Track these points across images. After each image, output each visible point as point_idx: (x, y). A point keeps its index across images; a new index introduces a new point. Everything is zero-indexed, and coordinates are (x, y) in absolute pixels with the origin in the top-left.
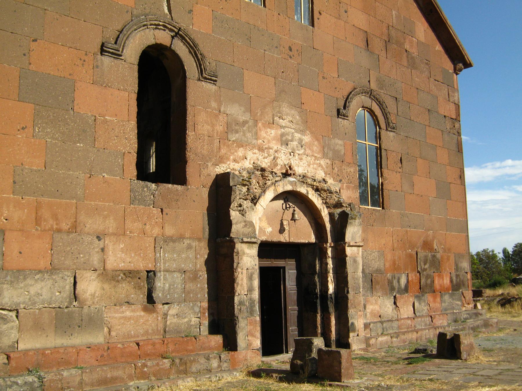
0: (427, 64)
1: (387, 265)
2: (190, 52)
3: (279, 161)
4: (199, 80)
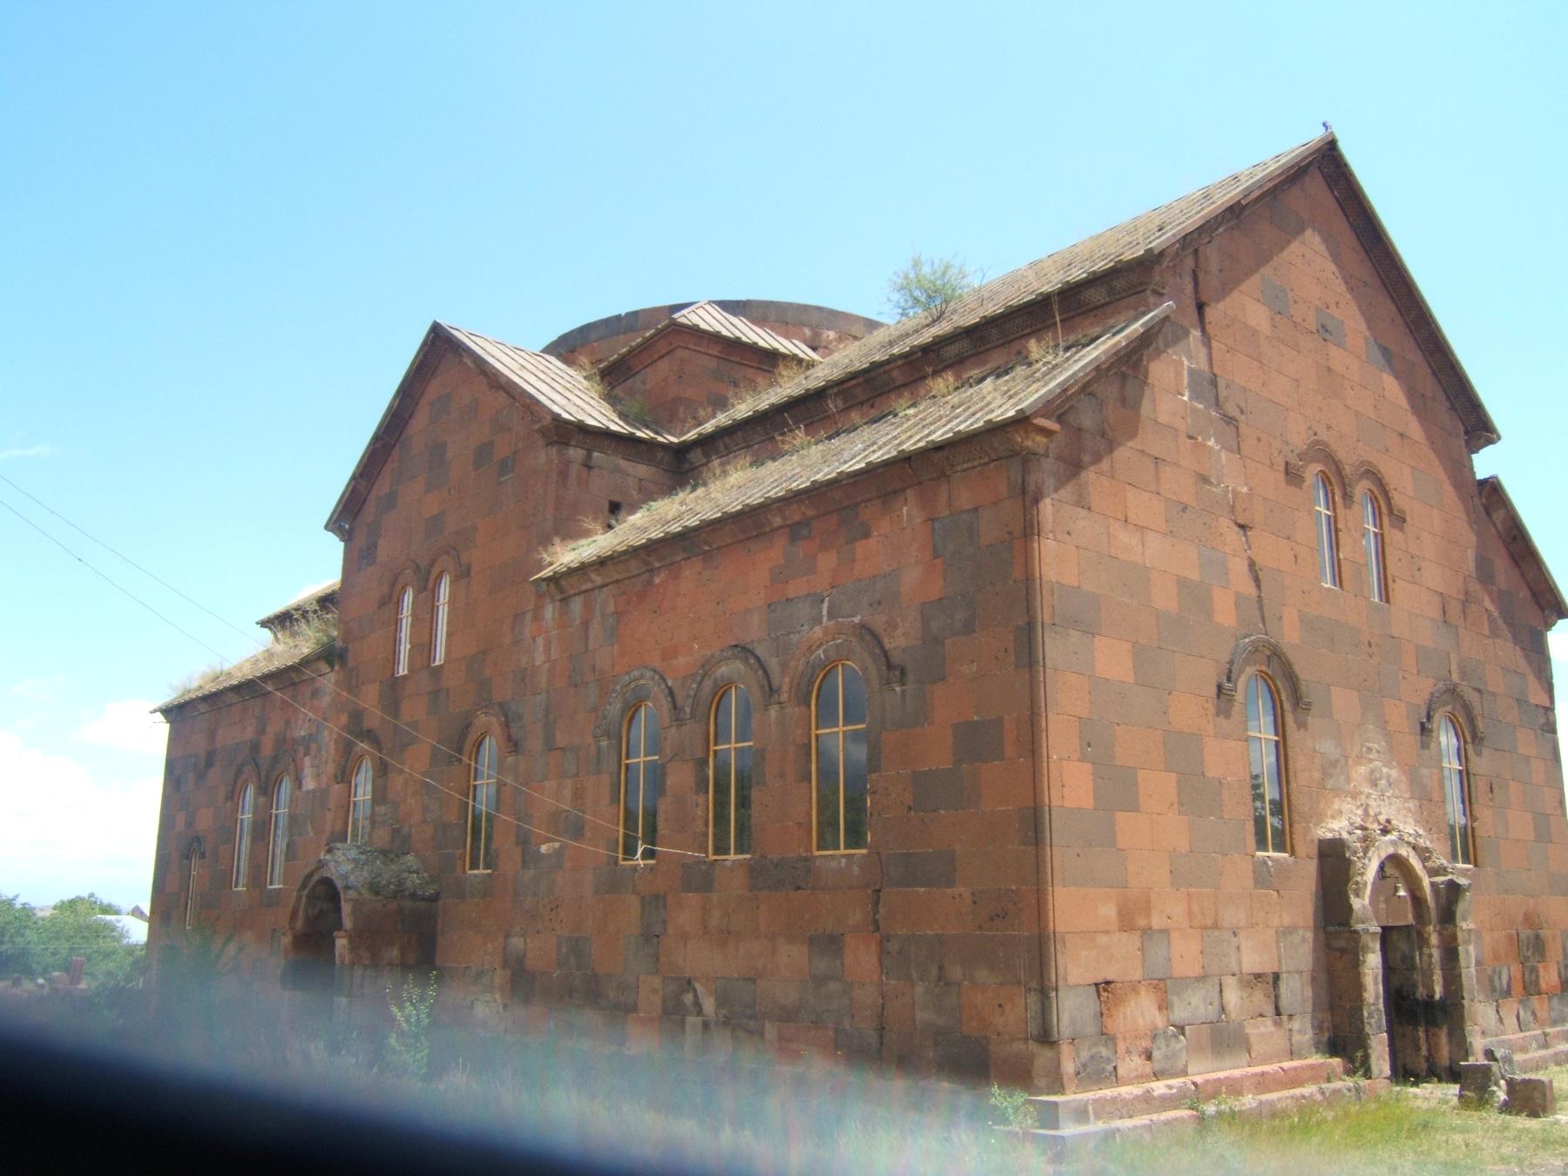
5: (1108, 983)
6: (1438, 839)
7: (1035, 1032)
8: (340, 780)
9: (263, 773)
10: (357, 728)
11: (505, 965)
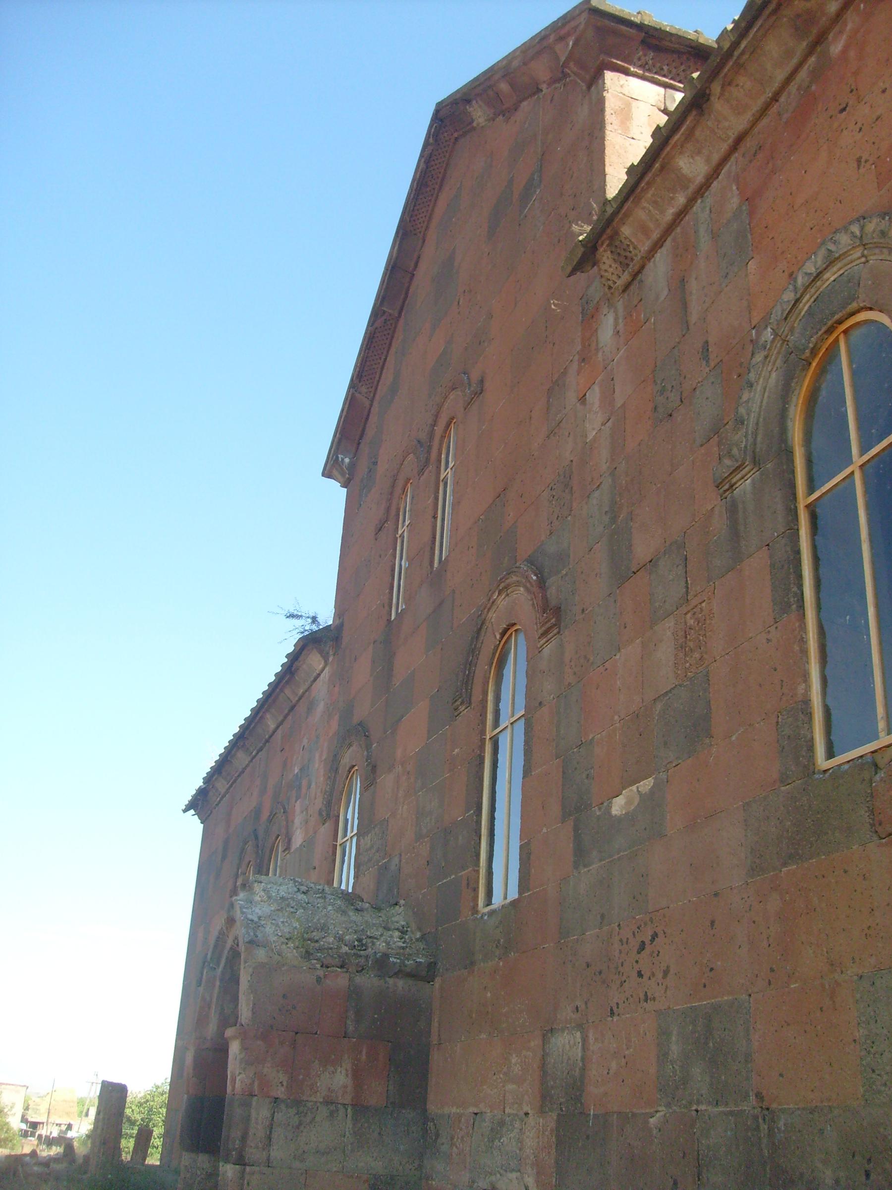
11: (545, 1099)
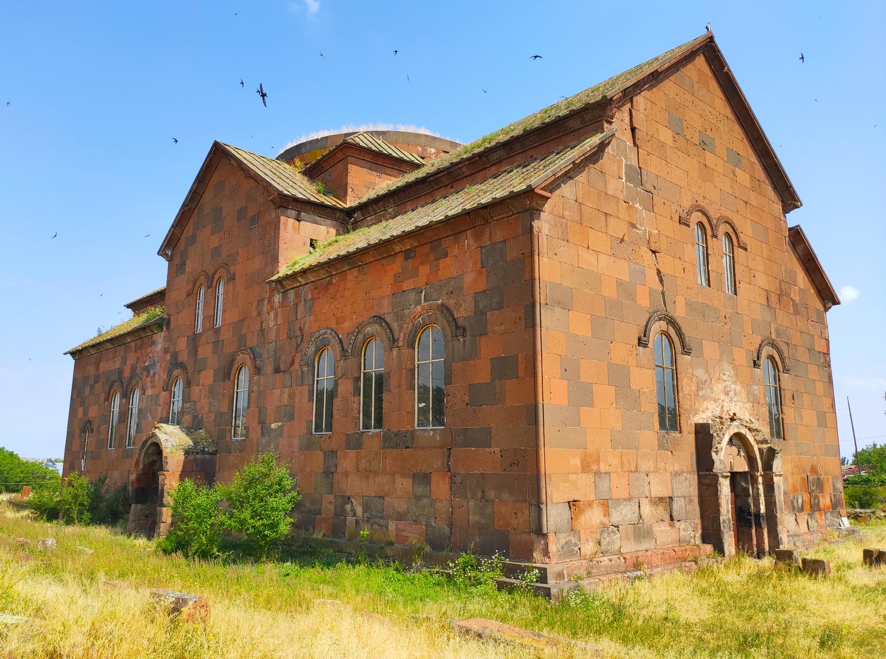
0: (805, 307)
1: (790, 487)
2: (677, 334)
3: (725, 409)
4: (682, 354)
5: (574, 501)
6: (763, 425)
7: (534, 529)
8: (165, 389)
9: (124, 386)
10: (176, 363)
